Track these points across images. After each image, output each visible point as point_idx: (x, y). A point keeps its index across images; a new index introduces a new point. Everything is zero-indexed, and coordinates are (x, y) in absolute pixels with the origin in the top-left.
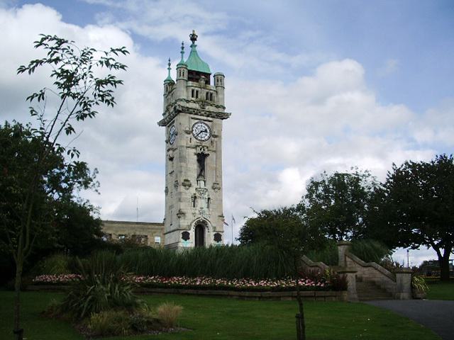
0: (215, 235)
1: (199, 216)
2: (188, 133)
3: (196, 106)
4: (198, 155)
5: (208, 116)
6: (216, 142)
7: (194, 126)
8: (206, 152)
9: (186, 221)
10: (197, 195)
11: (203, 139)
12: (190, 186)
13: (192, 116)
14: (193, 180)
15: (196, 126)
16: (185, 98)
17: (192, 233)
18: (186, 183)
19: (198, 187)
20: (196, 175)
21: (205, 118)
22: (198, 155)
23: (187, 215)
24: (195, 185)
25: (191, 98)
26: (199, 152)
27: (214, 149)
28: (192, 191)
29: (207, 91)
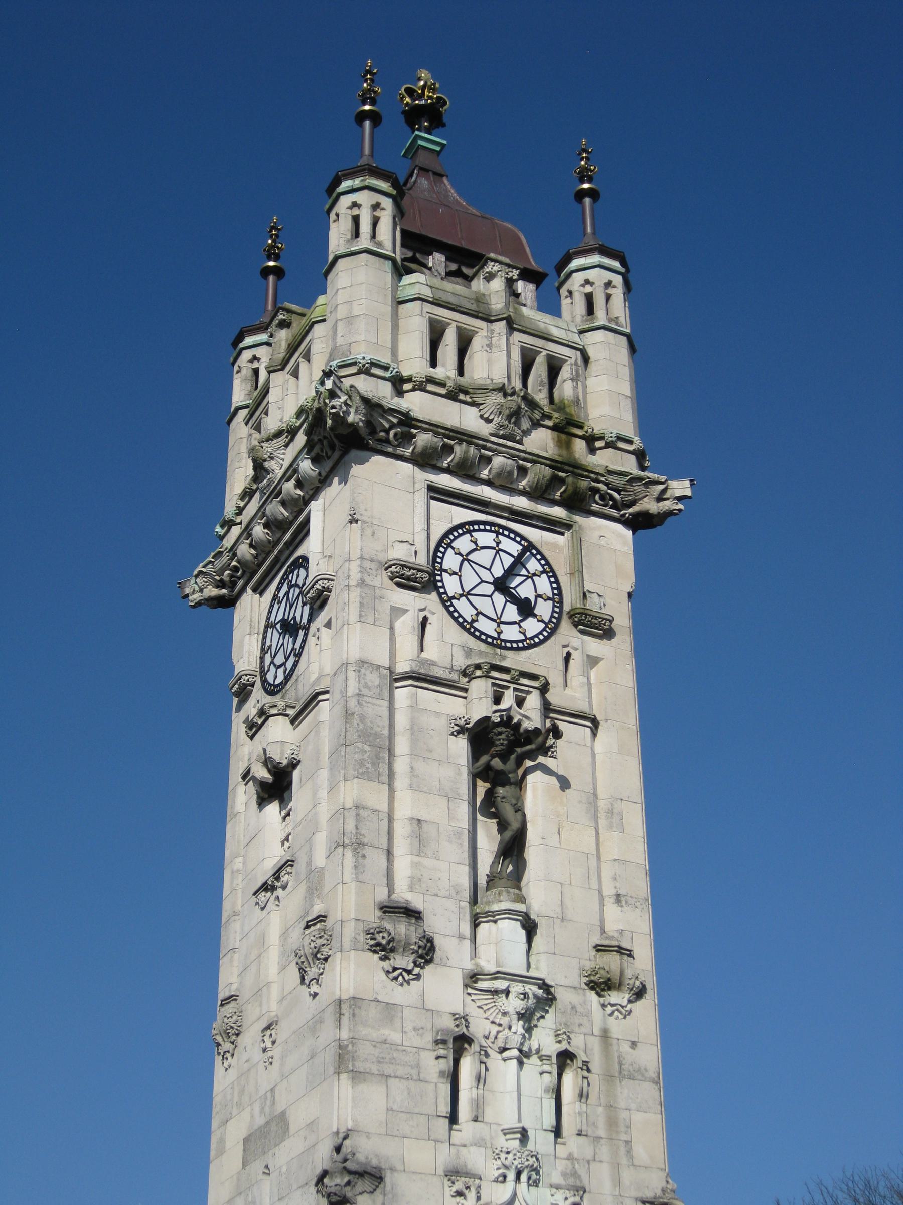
3: (467, 418)
4: (480, 736)
5: (538, 493)
6: (593, 661)
10: (479, 1027)
11: (511, 633)
13: (446, 481)
15: (463, 543)
18: (401, 929)
21: (521, 503)
23: (388, 1178)
24: (454, 954)
25: (414, 364)
26: (478, 705)
28: (441, 990)
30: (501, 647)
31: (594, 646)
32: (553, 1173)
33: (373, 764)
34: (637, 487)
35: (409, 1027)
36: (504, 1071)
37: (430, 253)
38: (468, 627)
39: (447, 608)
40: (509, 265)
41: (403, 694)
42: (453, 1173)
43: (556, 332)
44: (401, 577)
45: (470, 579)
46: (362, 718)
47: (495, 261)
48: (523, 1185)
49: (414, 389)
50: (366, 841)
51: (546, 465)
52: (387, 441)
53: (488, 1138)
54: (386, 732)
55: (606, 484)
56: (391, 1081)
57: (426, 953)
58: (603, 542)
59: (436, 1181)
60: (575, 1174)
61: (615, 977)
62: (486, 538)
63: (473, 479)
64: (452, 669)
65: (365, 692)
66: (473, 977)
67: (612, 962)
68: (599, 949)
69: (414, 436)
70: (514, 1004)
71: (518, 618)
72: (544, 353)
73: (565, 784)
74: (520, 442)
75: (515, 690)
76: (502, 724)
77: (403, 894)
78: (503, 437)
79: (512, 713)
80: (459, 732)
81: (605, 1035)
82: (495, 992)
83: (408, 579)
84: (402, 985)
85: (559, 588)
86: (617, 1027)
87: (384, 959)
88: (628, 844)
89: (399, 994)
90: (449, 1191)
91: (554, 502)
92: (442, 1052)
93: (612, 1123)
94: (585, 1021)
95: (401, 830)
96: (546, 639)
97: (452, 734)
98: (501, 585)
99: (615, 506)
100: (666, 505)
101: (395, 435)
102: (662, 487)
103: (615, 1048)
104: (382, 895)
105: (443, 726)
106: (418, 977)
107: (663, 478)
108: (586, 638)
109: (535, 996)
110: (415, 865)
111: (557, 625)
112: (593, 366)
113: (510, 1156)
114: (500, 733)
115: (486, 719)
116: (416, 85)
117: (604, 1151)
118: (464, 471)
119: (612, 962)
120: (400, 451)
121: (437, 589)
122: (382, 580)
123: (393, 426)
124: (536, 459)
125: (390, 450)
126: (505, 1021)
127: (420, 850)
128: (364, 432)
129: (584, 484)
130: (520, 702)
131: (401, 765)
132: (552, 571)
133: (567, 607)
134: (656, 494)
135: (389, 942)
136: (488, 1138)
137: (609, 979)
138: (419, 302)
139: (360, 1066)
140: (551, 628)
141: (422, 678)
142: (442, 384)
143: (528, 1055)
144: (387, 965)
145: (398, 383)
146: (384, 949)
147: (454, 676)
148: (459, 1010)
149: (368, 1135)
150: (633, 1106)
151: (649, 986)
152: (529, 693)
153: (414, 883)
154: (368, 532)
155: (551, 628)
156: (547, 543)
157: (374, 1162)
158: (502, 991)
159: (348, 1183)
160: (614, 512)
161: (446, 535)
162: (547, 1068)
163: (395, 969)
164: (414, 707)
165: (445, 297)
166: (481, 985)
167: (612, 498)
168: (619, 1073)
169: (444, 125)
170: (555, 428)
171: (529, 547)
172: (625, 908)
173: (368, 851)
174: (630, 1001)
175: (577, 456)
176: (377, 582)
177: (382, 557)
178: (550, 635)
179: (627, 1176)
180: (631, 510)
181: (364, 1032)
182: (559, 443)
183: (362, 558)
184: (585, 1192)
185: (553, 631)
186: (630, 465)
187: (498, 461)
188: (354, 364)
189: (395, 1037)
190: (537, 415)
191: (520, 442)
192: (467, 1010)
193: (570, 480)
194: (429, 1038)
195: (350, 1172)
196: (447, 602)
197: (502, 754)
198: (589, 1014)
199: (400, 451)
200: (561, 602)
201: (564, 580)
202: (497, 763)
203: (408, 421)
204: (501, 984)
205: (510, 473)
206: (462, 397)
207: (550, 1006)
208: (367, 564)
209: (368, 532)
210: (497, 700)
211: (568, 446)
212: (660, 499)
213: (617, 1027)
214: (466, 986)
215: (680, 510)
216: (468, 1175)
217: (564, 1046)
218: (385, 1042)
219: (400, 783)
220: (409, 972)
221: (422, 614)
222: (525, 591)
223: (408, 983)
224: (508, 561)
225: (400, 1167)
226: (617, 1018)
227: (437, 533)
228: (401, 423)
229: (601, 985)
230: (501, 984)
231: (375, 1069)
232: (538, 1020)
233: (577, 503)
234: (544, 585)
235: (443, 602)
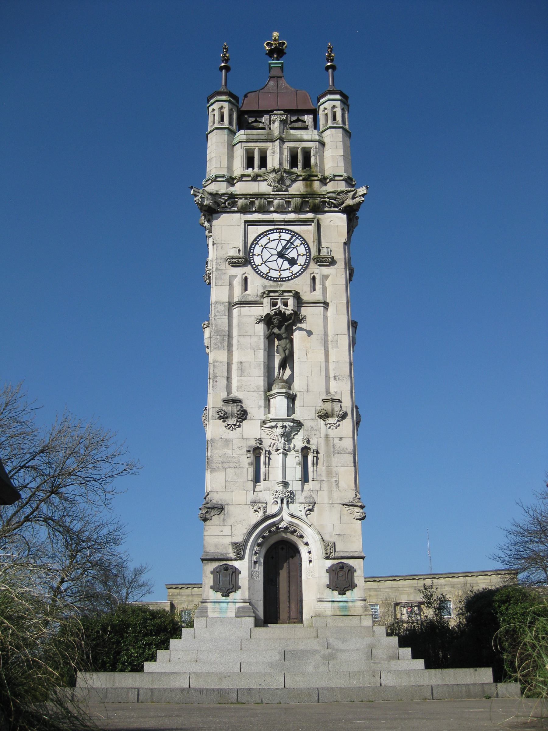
0: (330, 570)
1: (272, 509)
2: (235, 263)
3: (263, 187)
5: (299, 210)
8: (289, 310)
9: (227, 530)
11: (286, 274)
12: (243, 415)
14: (253, 402)
15: (263, 241)
16: (224, 172)
17: (248, 570)
18: (231, 408)
19: (271, 416)
20: (258, 380)
22: (268, 320)
26: (265, 309)
28: (251, 430)
29: (292, 144)
30: (280, 281)
31: (326, 270)
32: (300, 497)
33: (221, 343)
34: (343, 196)
35: (235, 447)
36: (277, 458)
37: (262, 116)
38: (266, 277)
39: (255, 270)
40: (281, 114)
42: (254, 503)
43: (305, 137)
44: (232, 263)
45: (266, 255)
46: (216, 325)
47: (275, 114)
48: (285, 505)
49: (237, 182)
50: (217, 375)
51: (298, 197)
52: (226, 207)
53: (270, 487)
54: (227, 329)
55: (328, 198)
56: (227, 469)
57: (243, 415)
58: (332, 223)
59: (247, 507)
60: (311, 497)
61: (330, 412)
62: (275, 236)
63: (268, 212)
64: (257, 296)
65: (217, 314)
66: (264, 422)
67: (328, 406)
68: (325, 401)
69: (237, 202)
70: (279, 431)
71: (289, 266)
72: (301, 147)
73: (310, 333)
74: (287, 191)
75: (282, 299)
76: (276, 314)
77: (235, 394)
78: (277, 191)
79: (281, 309)
80: (259, 322)
81: (327, 437)
82: (272, 427)
83: (235, 263)
84: (232, 430)
85: (309, 249)
87: (224, 421)
88: (341, 353)
89: (231, 434)
90: (252, 511)
91: (307, 212)
92: (249, 455)
93: (329, 473)
94: (317, 432)
95: (235, 367)
96: (302, 272)
97: (256, 323)
99: (335, 206)
100: (357, 200)
101: (229, 204)
102: (353, 192)
103: (332, 441)
104: (224, 395)
105: (253, 320)
106: (239, 426)
107: (353, 189)
108: (322, 268)
109: (289, 426)
110: (239, 381)
111: (308, 265)
112: (327, 147)
113: (277, 494)
114: (274, 319)
115: (268, 314)
116: (271, 40)
117: (325, 486)
118: (262, 210)
119: (328, 406)
120: (233, 209)
121: (250, 263)
123: (226, 201)
124: (294, 196)
125: (228, 210)
126: (276, 438)
127: (241, 374)
128: (214, 206)
129: (317, 201)
130: (286, 304)
131: (235, 341)
132: (306, 242)
133: (312, 256)
134: (351, 196)
135: (224, 415)
136: (270, 487)
137: (327, 413)
138: (240, 143)
139: (214, 466)
140: (305, 267)
141: (241, 303)
142: (249, 176)
143: (289, 451)
144: (225, 424)
145: (231, 181)
146: (224, 417)
147: (258, 299)
148: (258, 437)
149: (217, 492)
150: (340, 465)
151: (349, 413)
152: (288, 299)
153: (239, 388)
154: (220, 247)
155: (305, 267)
156: (304, 231)
157: (220, 503)
158: (274, 427)
159: (207, 512)
160: (336, 209)
161: (255, 240)
162: (297, 455)
163: (228, 425)
164: (239, 316)
165: (251, 137)
166: (267, 425)
167: (333, 203)
168: (334, 451)
169: (285, 53)
170: (304, 180)
171: (295, 234)
172: (338, 381)
173: (218, 379)
174: (338, 421)
175: (315, 189)
176: (223, 267)
177: (225, 256)
178: (304, 270)
179: (336, 494)
180: (342, 206)
181: (216, 452)
182: (306, 186)
183: (217, 259)
184: (315, 503)
185: (306, 268)
186: (342, 186)
187: (276, 202)
188: (210, 179)
189: (229, 452)
190: (294, 177)
191: (287, 191)
192: (262, 436)
193: (311, 201)
194: (245, 450)
195: (208, 508)
196: (255, 268)
197: (281, 326)
198: (319, 430)
199: (233, 209)
200: (310, 255)
201: (311, 245)
202: (276, 331)
203: (232, 196)
204: (273, 424)
205: (283, 205)
206: (259, 179)
207: (300, 429)
208: (219, 261)
209: (220, 247)
210: (275, 304)
211: (311, 186)
212: (354, 198)
213: (333, 433)
214: (261, 426)
215: (363, 201)
216: (260, 503)
217: (306, 444)
218: (225, 454)
219: (234, 348)
220: (235, 425)
221: (244, 276)
222: (292, 254)
223: (235, 429)
224: (284, 243)
225: (231, 503)
226: (333, 429)
227: (251, 239)
228: (229, 198)
229: (324, 416)
230: (273, 424)
231: (220, 466)
232: (294, 435)
233: (317, 209)
234: (302, 249)
235: (253, 268)
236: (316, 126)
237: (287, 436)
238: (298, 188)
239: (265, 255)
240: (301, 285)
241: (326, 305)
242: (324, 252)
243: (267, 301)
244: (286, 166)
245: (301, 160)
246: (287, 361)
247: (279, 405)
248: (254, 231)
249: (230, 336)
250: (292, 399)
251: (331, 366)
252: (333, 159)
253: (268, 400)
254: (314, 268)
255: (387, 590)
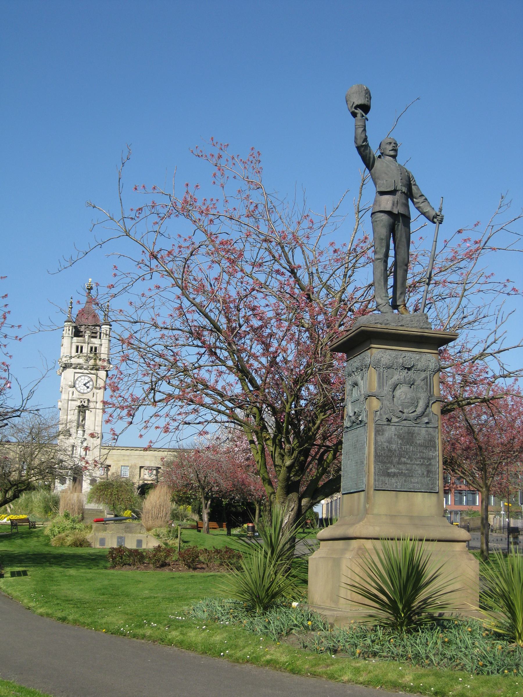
3: (81, 361)
5: (92, 369)
7: (77, 379)
8: (86, 404)
11: (85, 391)
15: (79, 379)
16: (69, 354)
22: (79, 407)
26: (79, 404)
27: (95, 400)
31: (98, 391)
38: (79, 392)
41: (70, 402)
45: (80, 384)
62: (83, 378)
70: (80, 441)
86: (95, 442)
98: (85, 385)
122: (67, 387)
129: (98, 367)
130: (85, 402)
141: (71, 400)
164: (71, 404)
222: (88, 385)
233: (97, 370)
236: (100, 338)
237: (82, 443)
238: (92, 362)
239: (80, 385)
240: (89, 396)
241: (97, 402)
242: (98, 386)
243: (79, 401)
244: (89, 352)
245: (94, 350)
246: (84, 419)
247: (80, 432)
248: (77, 375)
249: (67, 410)
250: (84, 431)
251: (96, 422)
252: (104, 350)
253: (77, 431)
254: (95, 390)
255: (136, 457)
